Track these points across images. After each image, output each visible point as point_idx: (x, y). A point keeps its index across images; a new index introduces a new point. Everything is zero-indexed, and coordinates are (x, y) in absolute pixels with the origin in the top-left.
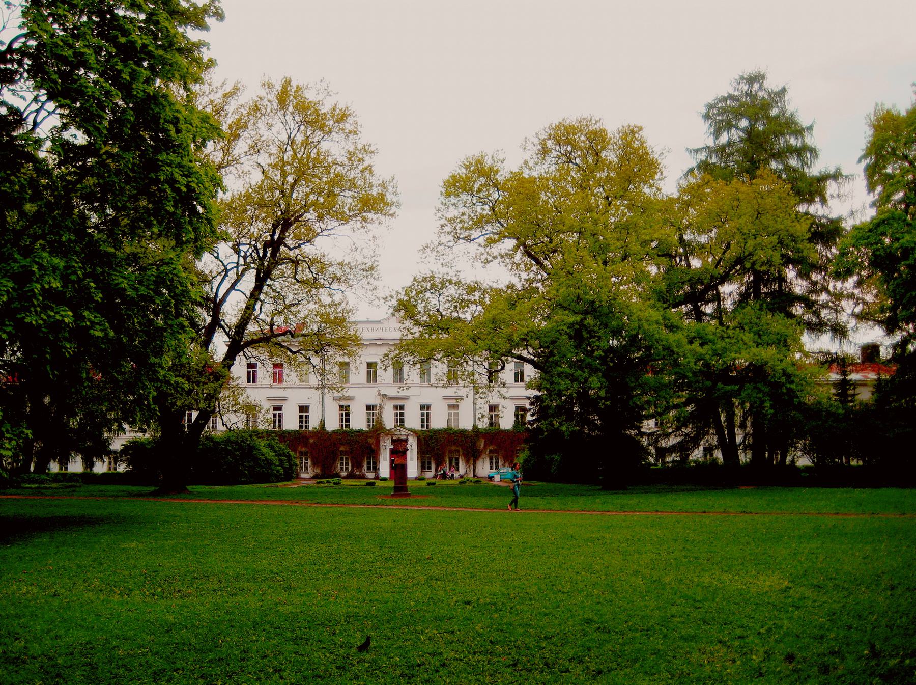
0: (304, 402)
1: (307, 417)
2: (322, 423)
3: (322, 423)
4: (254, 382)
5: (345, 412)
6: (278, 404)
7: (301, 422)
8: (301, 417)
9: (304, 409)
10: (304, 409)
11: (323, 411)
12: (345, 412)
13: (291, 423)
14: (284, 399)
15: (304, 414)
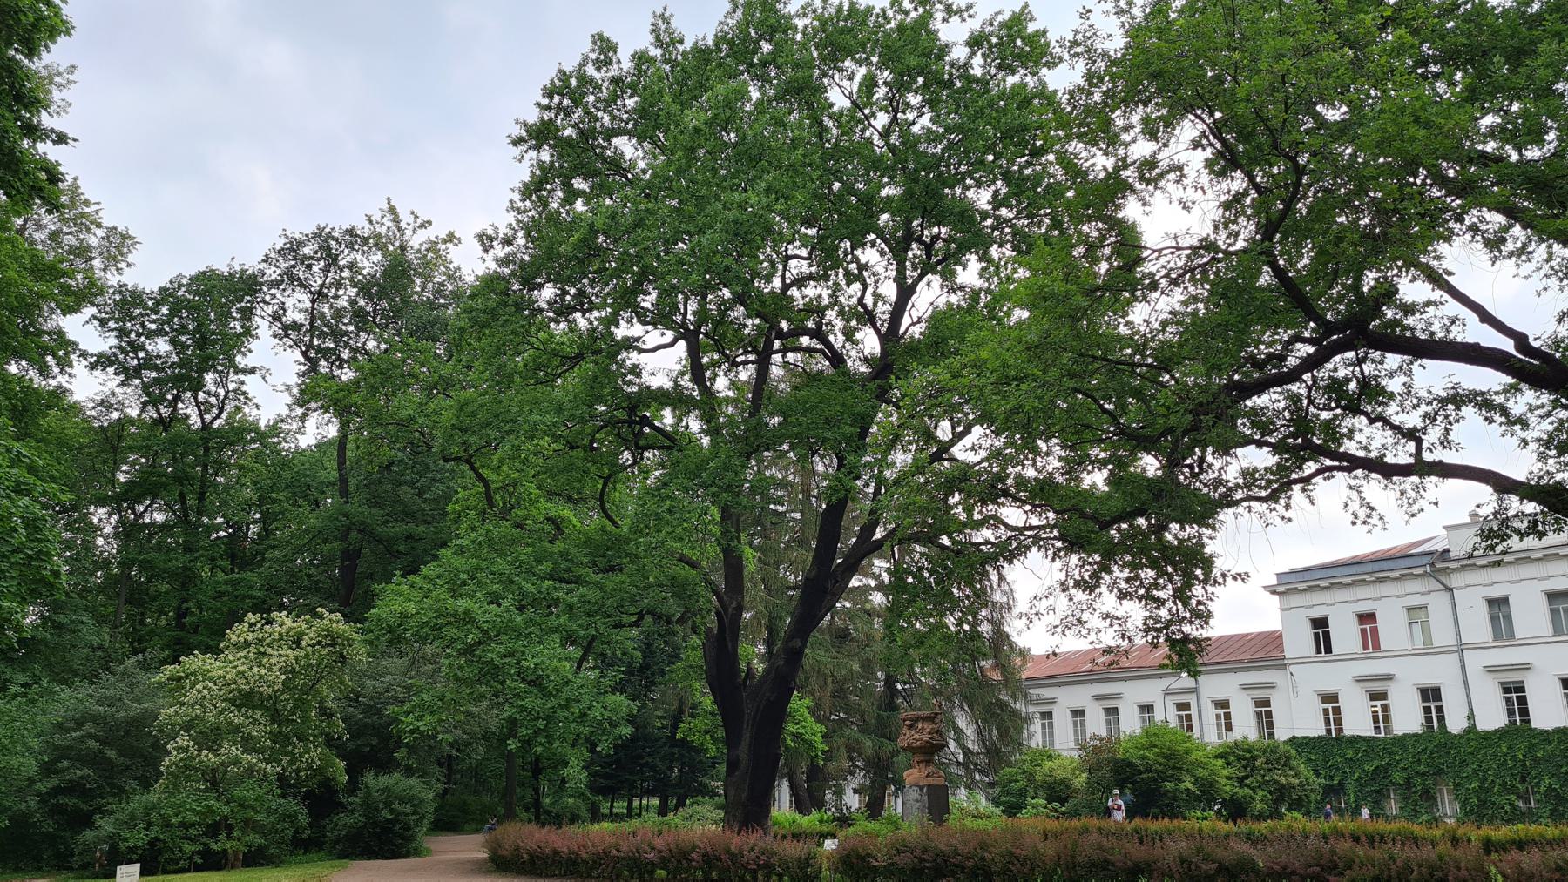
0: (1428, 681)
1: (1440, 709)
2: (1471, 716)
3: (1471, 716)
4: (1329, 650)
5: (1515, 695)
6: (1377, 687)
7: (1429, 720)
8: (1427, 710)
9: (1431, 694)
10: (1431, 694)
11: (1468, 696)
12: (1515, 695)
13: (1407, 719)
14: (1389, 678)
15: (1433, 705)
